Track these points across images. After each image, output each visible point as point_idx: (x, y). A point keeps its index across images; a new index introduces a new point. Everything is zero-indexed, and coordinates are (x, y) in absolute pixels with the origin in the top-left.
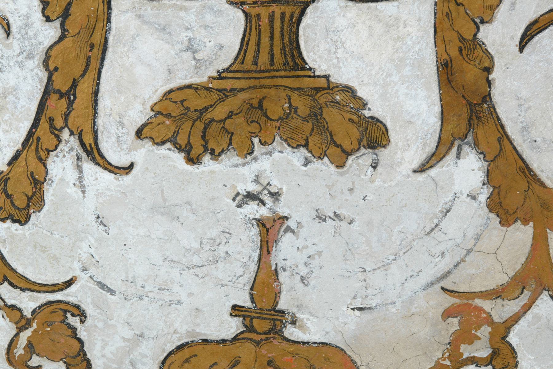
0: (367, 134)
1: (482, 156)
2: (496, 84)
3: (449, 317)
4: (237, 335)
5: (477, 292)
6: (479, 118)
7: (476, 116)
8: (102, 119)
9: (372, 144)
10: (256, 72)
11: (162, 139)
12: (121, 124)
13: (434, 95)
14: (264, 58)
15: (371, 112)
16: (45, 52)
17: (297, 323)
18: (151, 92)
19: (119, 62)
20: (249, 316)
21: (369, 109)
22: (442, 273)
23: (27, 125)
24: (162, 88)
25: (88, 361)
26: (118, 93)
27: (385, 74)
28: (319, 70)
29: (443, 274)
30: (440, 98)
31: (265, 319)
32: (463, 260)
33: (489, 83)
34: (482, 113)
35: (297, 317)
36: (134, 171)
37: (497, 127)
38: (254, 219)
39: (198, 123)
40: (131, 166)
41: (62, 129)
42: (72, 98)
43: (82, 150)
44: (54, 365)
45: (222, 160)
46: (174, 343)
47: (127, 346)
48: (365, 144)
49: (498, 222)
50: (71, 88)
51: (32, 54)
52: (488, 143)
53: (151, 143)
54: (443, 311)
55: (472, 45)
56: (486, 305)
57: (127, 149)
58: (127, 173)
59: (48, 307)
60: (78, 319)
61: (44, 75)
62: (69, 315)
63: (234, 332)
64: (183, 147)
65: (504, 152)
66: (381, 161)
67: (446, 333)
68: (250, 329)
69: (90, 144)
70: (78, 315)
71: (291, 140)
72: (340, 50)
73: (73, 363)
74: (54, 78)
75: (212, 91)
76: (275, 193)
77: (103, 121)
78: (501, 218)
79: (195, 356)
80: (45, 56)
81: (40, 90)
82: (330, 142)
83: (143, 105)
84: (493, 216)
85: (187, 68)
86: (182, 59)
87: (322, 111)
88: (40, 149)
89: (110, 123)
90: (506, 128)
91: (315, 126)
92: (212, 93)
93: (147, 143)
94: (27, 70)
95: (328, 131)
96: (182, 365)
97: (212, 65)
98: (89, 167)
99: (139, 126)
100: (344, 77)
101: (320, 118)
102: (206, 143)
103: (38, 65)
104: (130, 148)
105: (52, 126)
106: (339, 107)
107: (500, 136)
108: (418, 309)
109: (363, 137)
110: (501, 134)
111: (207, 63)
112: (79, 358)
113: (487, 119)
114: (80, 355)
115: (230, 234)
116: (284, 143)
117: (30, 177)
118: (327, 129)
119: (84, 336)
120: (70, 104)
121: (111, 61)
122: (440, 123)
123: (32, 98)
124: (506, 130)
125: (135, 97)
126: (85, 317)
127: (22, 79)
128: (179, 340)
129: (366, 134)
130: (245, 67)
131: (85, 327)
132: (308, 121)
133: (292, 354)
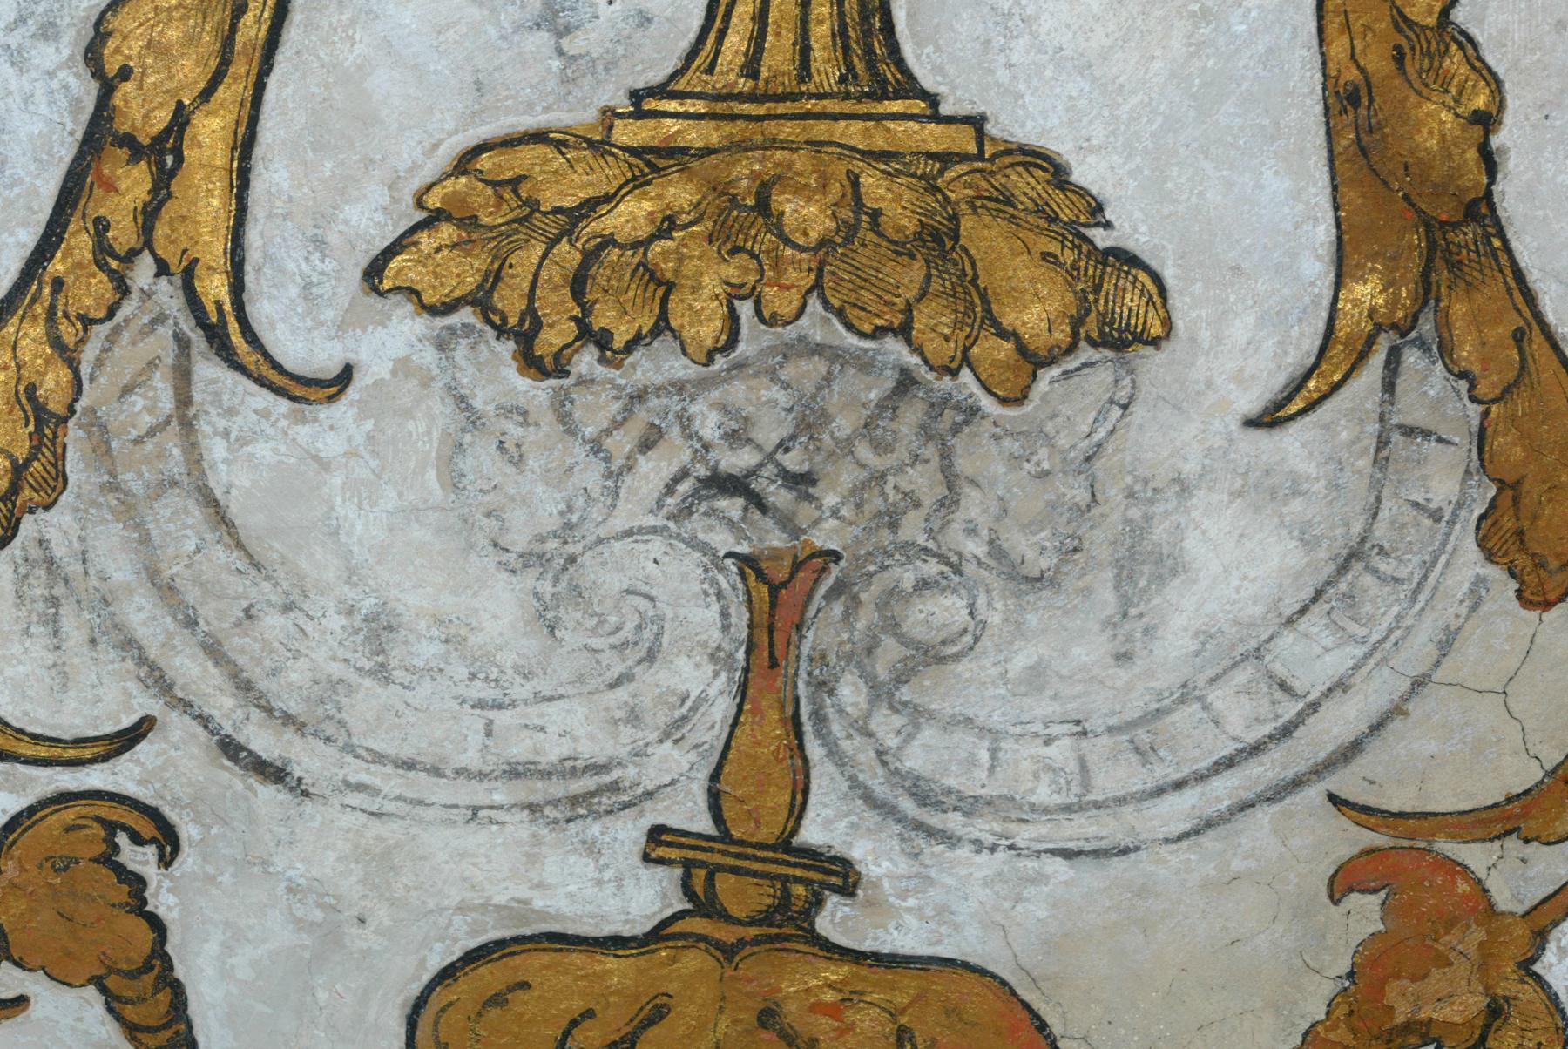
0: (1102, 301)
1: (1463, 385)
2: (1511, 164)
3: (1352, 890)
4: (664, 924)
5: (1444, 814)
6: (1455, 266)
7: (1447, 261)
8: (259, 227)
9: (1116, 334)
10: (751, 97)
11: (448, 295)
12: (319, 243)
13: (1313, 190)
14: (778, 57)
15: (1115, 233)
16: (93, 19)
17: (860, 892)
18: (419, 150)
19: (322, 54)
20: (703, 864)
21: (1108, 225)
22: (1330, 748)
23: (28, 237)
24: (454, 139)
25: (177, 989)
26: (314, 150)
27: (1160, 120)
28: (951, 99)
29: (1334, 752)
30: (1334, 199)
31: (755, 874)
32: (1397, 710)
33: (1490, 161)
34: (1464, 252)
35: (859, 874)
36: (353, 393)
37: (1511, 295)
38: (729, 555)
39: (564, 245)
40: (345, 376)
41: (130, 256)
42: (169, 160)
43: (193, 322)
44: (69, 996)
45: (633, 366)
46: (456, 941)
47: (304, 947)
48: (1095, 335)
49: (1512, 594)
50: (167, 131)
51: (53, 24)
52: (1483, 344)
53: (410, 307)
54: (1332, 871)
55: (1434, 44)
56: (1475, 856)
57: (333, 322)
58: (331, 399)
59: (57, 811)
60: (151, 852)
61: (87, 91)
62: (122, 839)
63: (654, 914)
64: (513, 321)
65: (1534, 376)
66: (1144, 389)
67: (1342, 942)
68: (703, 904)
69: (219, 305)
70: (153, 841)
71: (856, 312)
72: (1021, 41)
73: (128, 994)
74: (117, 100)
75: (613, 154)
76: (802, 475)
77: (262, 235)
78: (1522, 583)
79: (525, 985)
80: (92, 33)
81: (71, 134)
82: (983, 322)
83: (390, 188)
84: (1495, 573)
85: (536, 80)
86: (520, 54)
87: (958, 226)
88: (60, 314)
89: (284, 239)
90: (1540, 303)
91: (934, 272)
92: (610, 159)
93: (398, 305)
94: (34, 74)
95: (977, 287)
96: (480, 1014)
97: (613, 72)
98: (209, 371)
99: (376, 252)
100: (1030, 124)
101: (953, 248)
102: (587, 310)
103: (71, 58)
104: (343, 322)
105: (103, 250)
106: (1013, 216)
107: (1522, 324)
108: (1252, 864)
109: (1088, 311)
110: (1525, 319)
111: (600, 68)
112: (149, 979)
113: (1481, 271)
114: (152, 968)
115: (652, 599)
116: (835, 321)
117: (24, 401)
118: (974, 281)
119: (169, 909)
120: (163, 183)
121: (297, 53)
122: (1332, 277)
123: (45, 157)
124: (1541, 308)
125: (368, 162)
126: (176, 849)
127: (18, 100)
128: (474, 932)
129: (1096, 301)
130: (718, 82)
131: (172, 879)
132: (912, 256)
133: (840, 991)
